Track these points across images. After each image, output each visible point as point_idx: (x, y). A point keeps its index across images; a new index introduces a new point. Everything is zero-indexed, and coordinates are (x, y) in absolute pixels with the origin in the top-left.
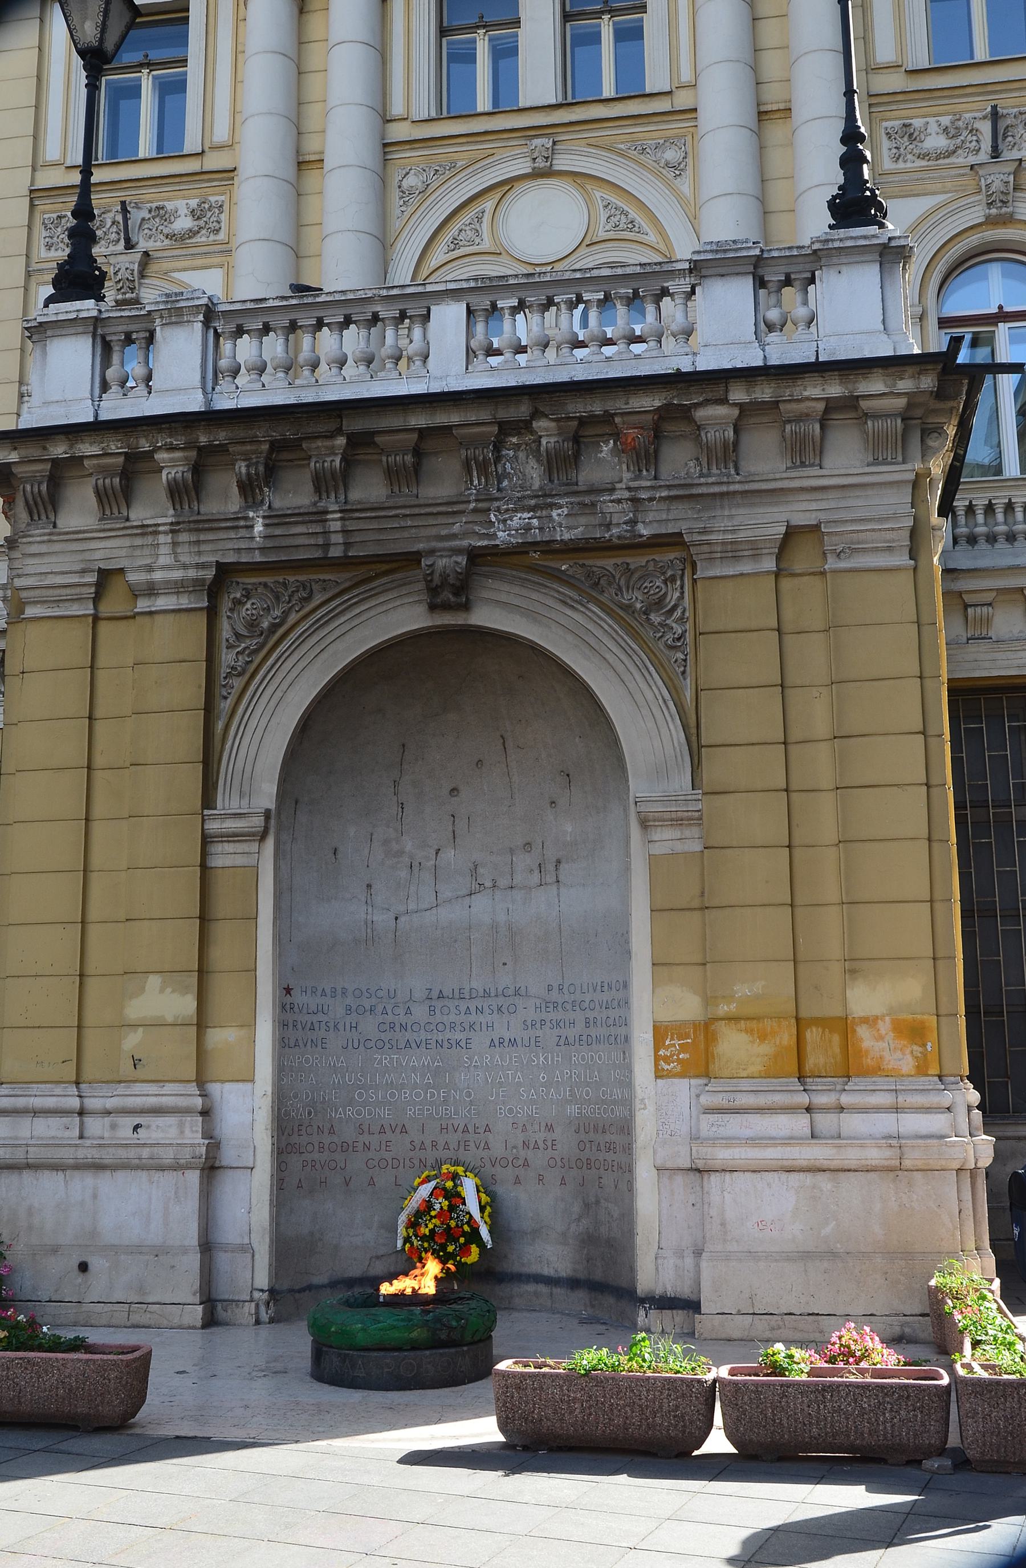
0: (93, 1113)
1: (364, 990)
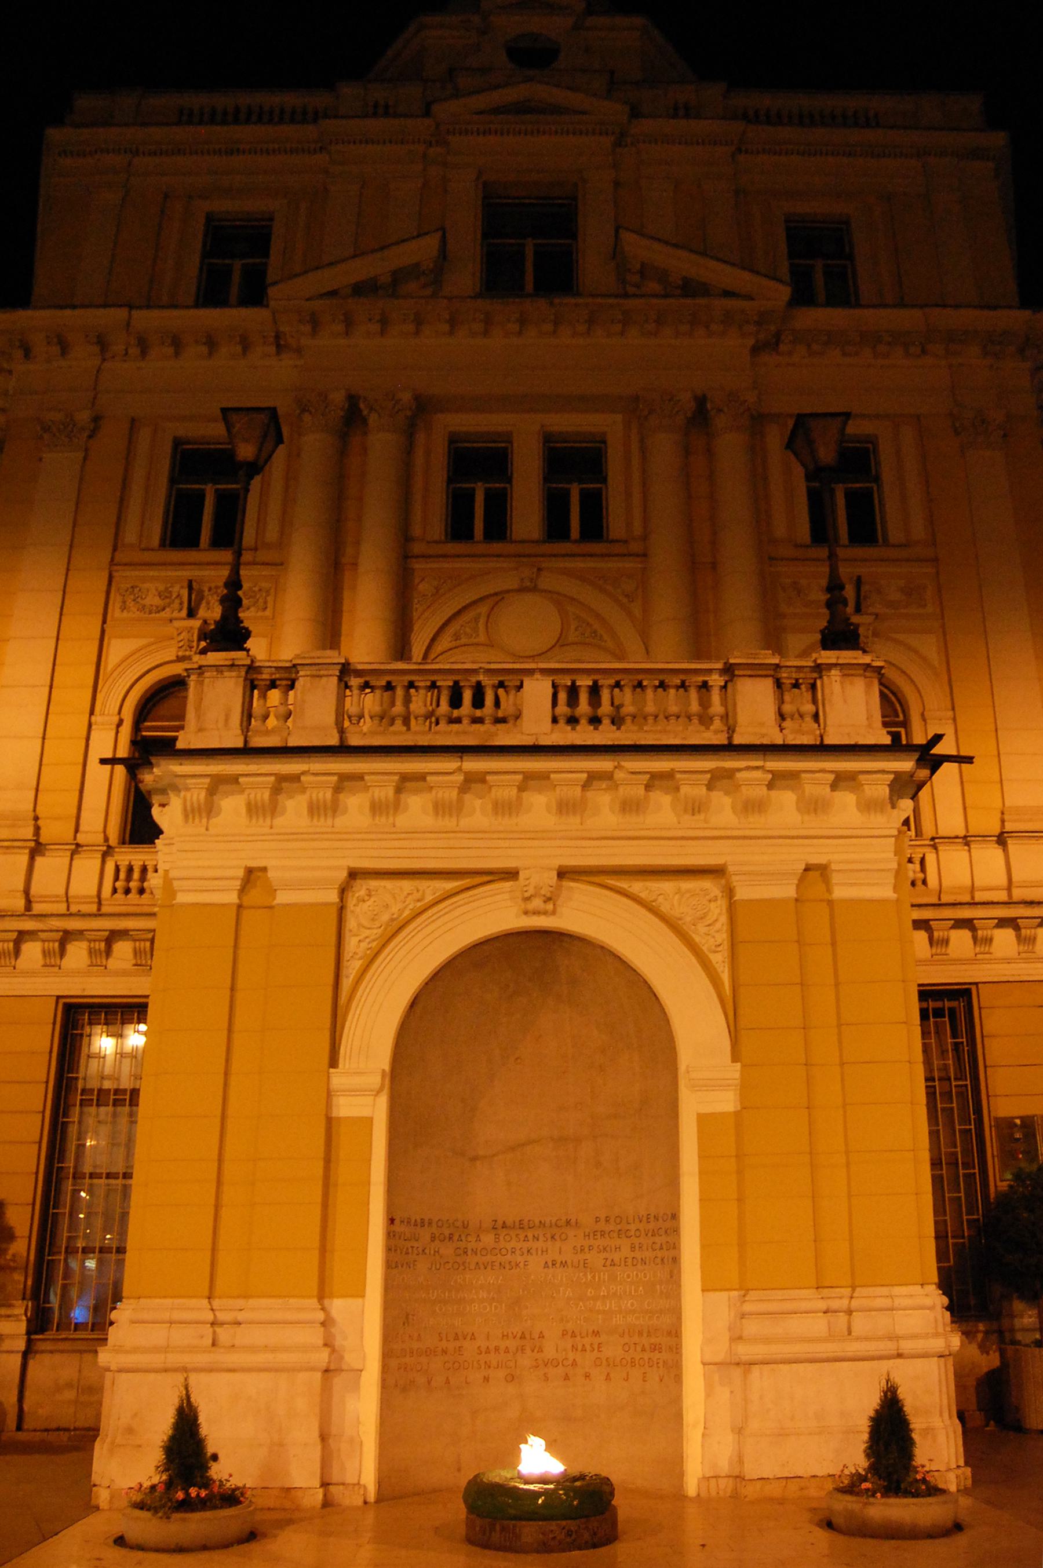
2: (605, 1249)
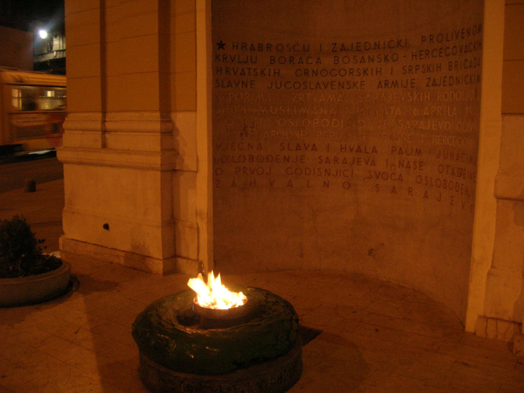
0: (109, 131)
2: (428, 68)
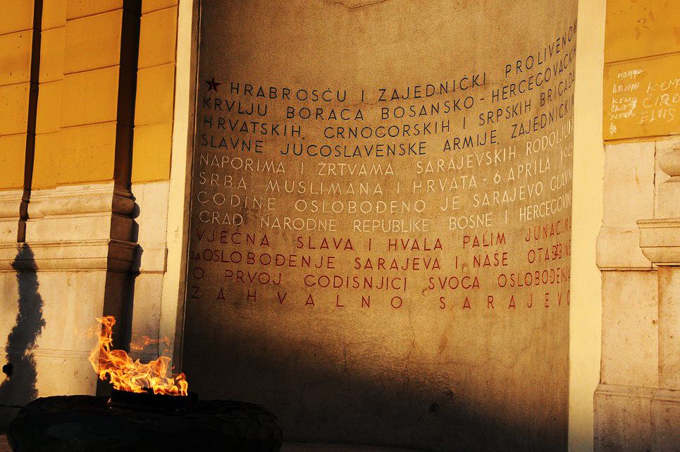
1: (310, 91)
